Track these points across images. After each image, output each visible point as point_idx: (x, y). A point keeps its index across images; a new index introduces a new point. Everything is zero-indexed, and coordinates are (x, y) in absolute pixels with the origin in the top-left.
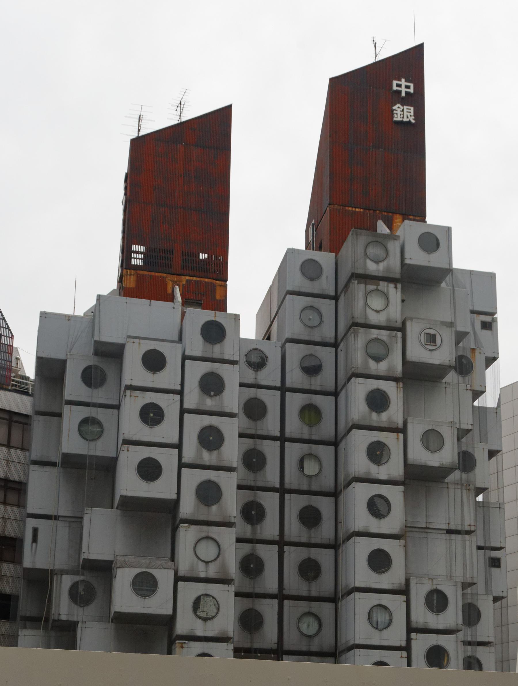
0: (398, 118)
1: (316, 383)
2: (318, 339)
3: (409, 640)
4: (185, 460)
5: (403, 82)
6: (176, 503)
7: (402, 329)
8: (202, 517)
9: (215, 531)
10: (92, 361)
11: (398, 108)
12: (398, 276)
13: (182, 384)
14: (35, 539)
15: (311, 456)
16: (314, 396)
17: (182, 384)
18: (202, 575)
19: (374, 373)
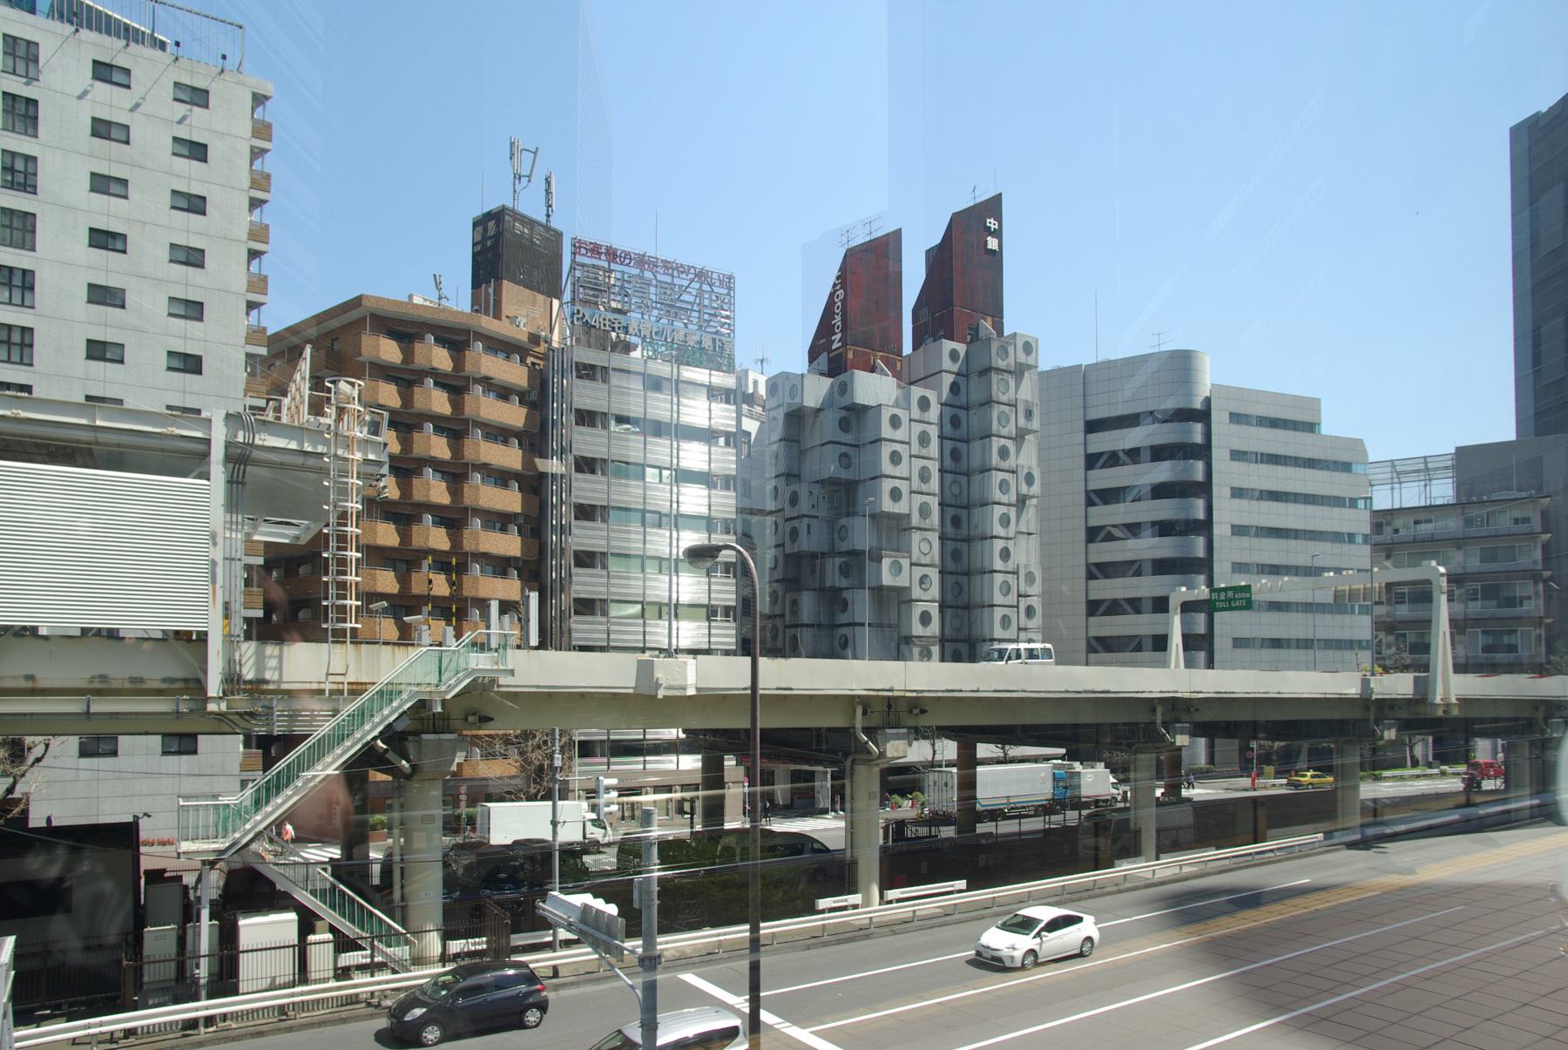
0: (989, 247)
1: (958, 434)
2: (958, 404)
3: (1018, 601)
4: (913, 489)
5: (992, 220)
6: (909, 516)
7: (1015, 406)
8: (922, 526)
9: (929, 535)
10: (844, 414)
11: (989, 238)
12: (1013, 370)
13: (910, 438)
14: (809, 532)
15: (955, 481)
16: (958, 443)
17: (910, 438)
18: (923, 562)
19: (1002, 434)
